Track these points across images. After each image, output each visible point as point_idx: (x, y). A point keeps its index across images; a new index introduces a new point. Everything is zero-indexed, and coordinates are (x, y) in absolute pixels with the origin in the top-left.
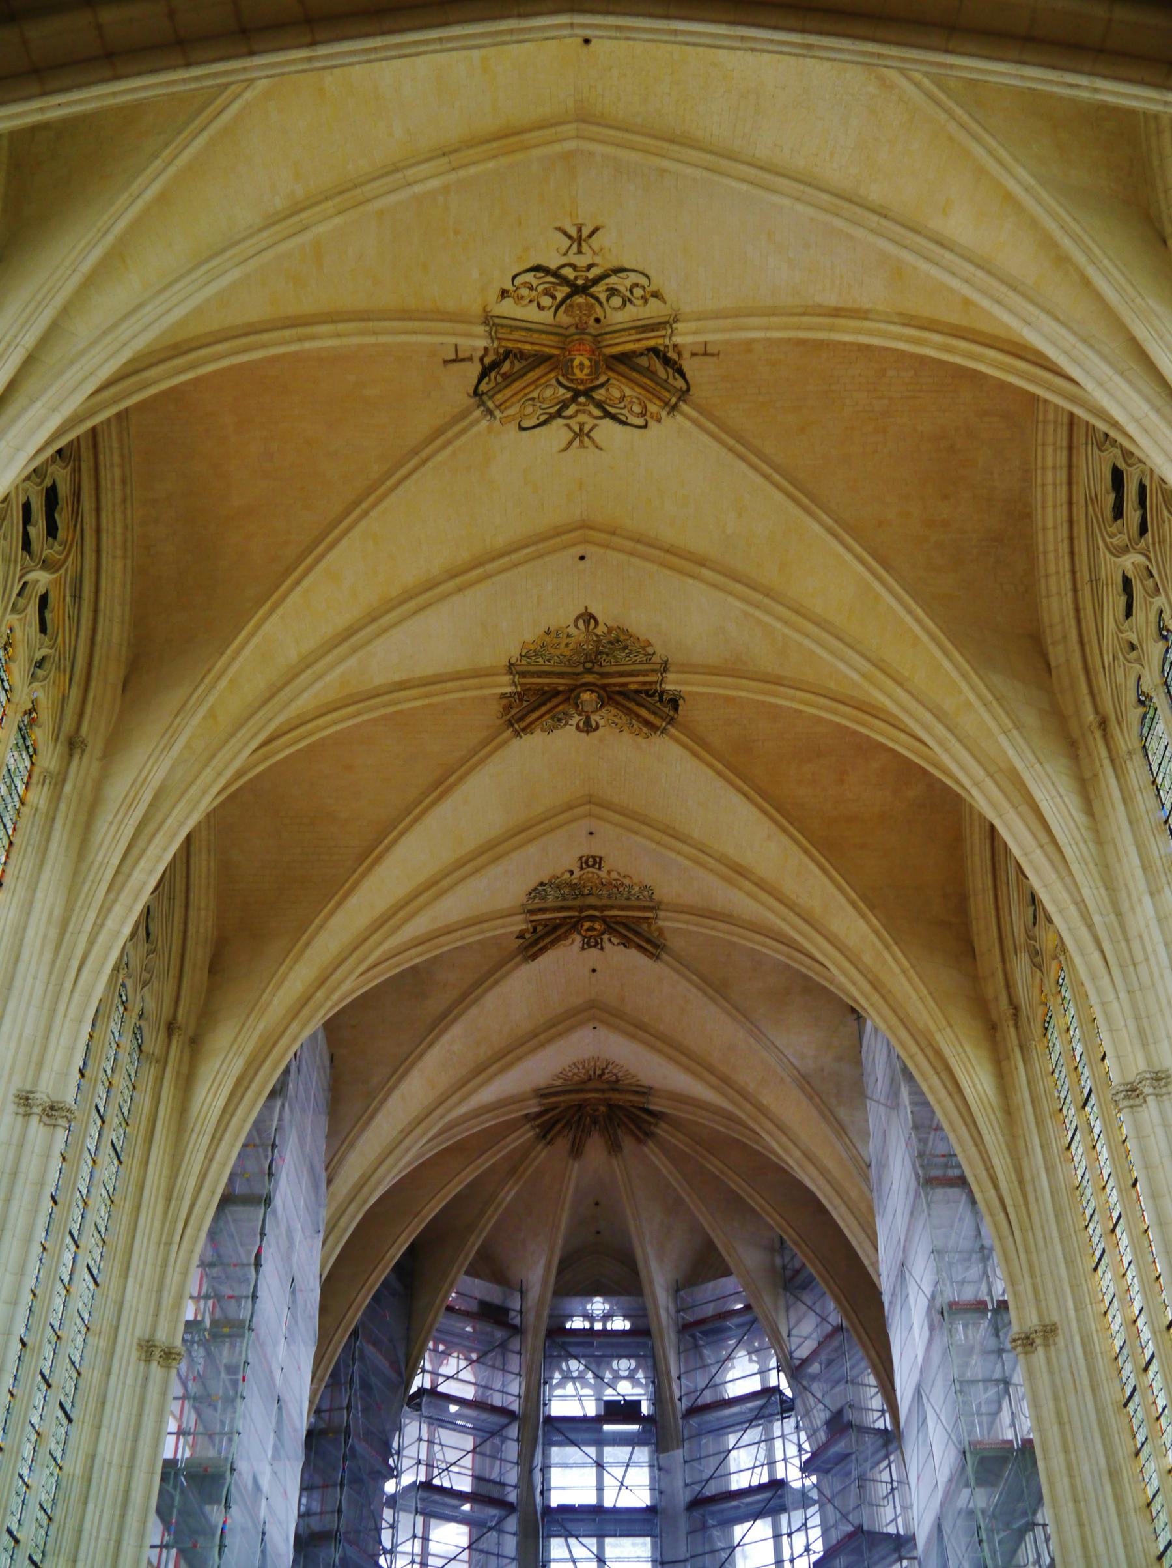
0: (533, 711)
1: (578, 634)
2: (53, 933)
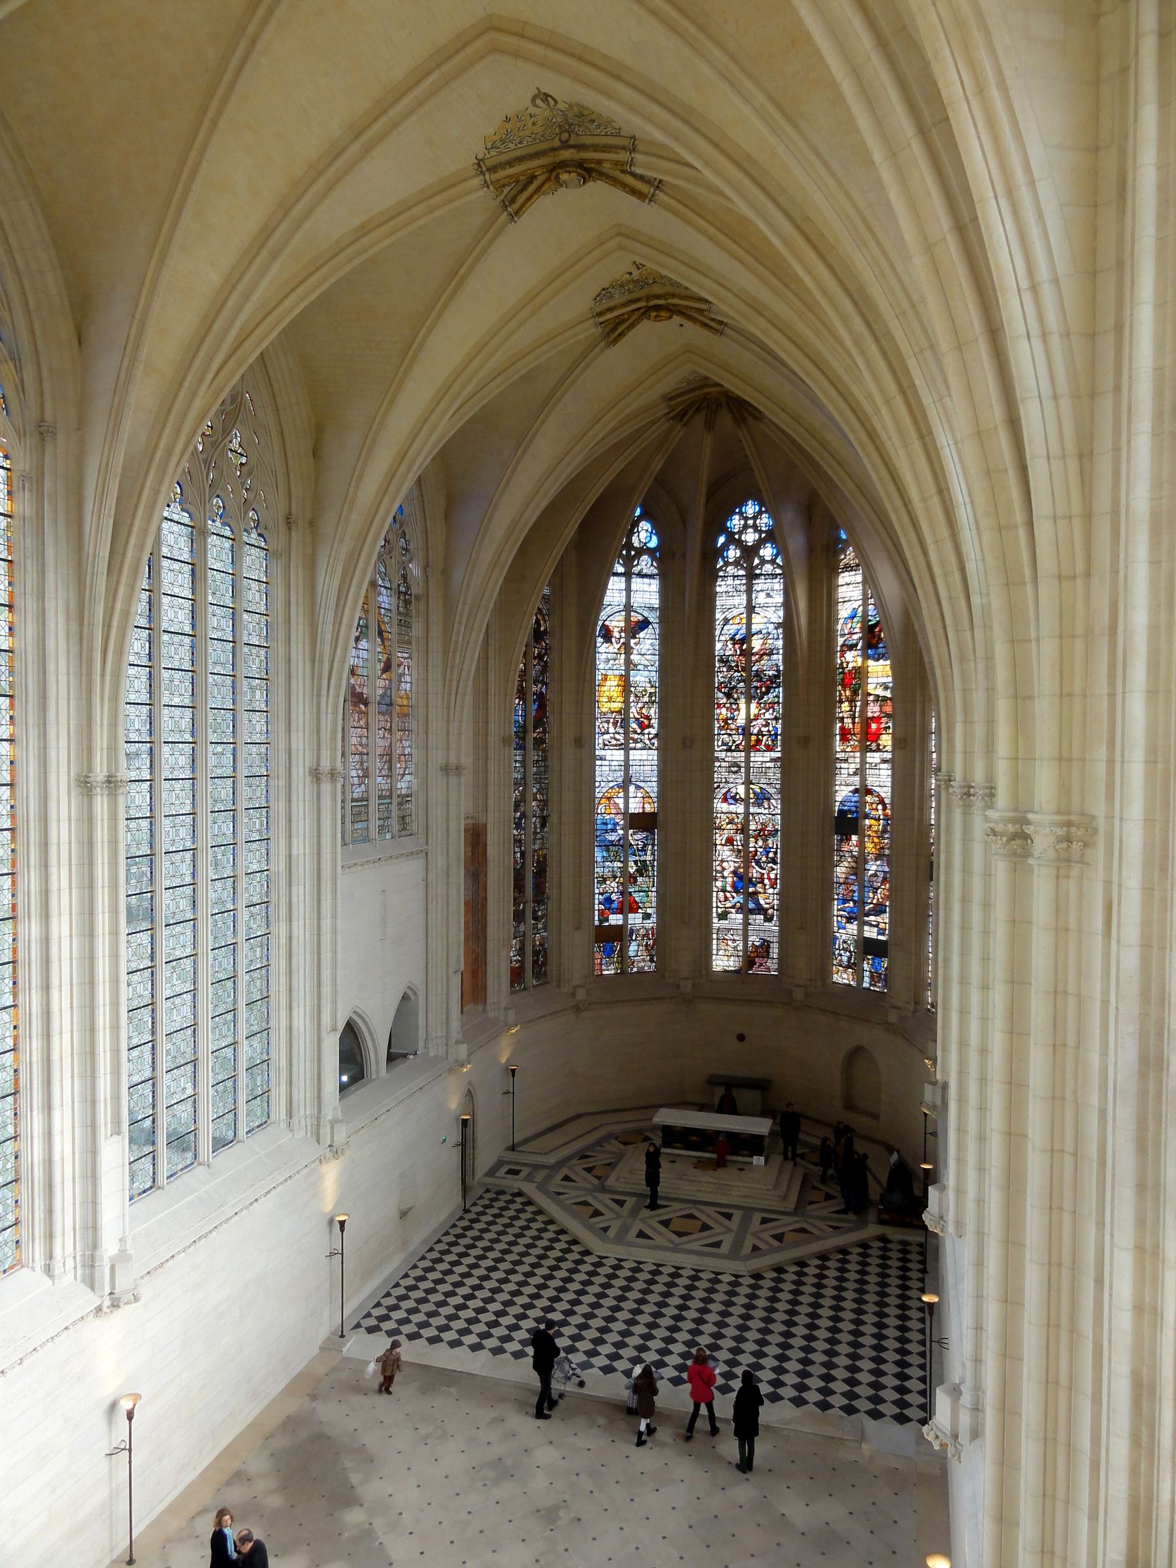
0: (521, 191)
1: (542, 111)
2: (74, 627)
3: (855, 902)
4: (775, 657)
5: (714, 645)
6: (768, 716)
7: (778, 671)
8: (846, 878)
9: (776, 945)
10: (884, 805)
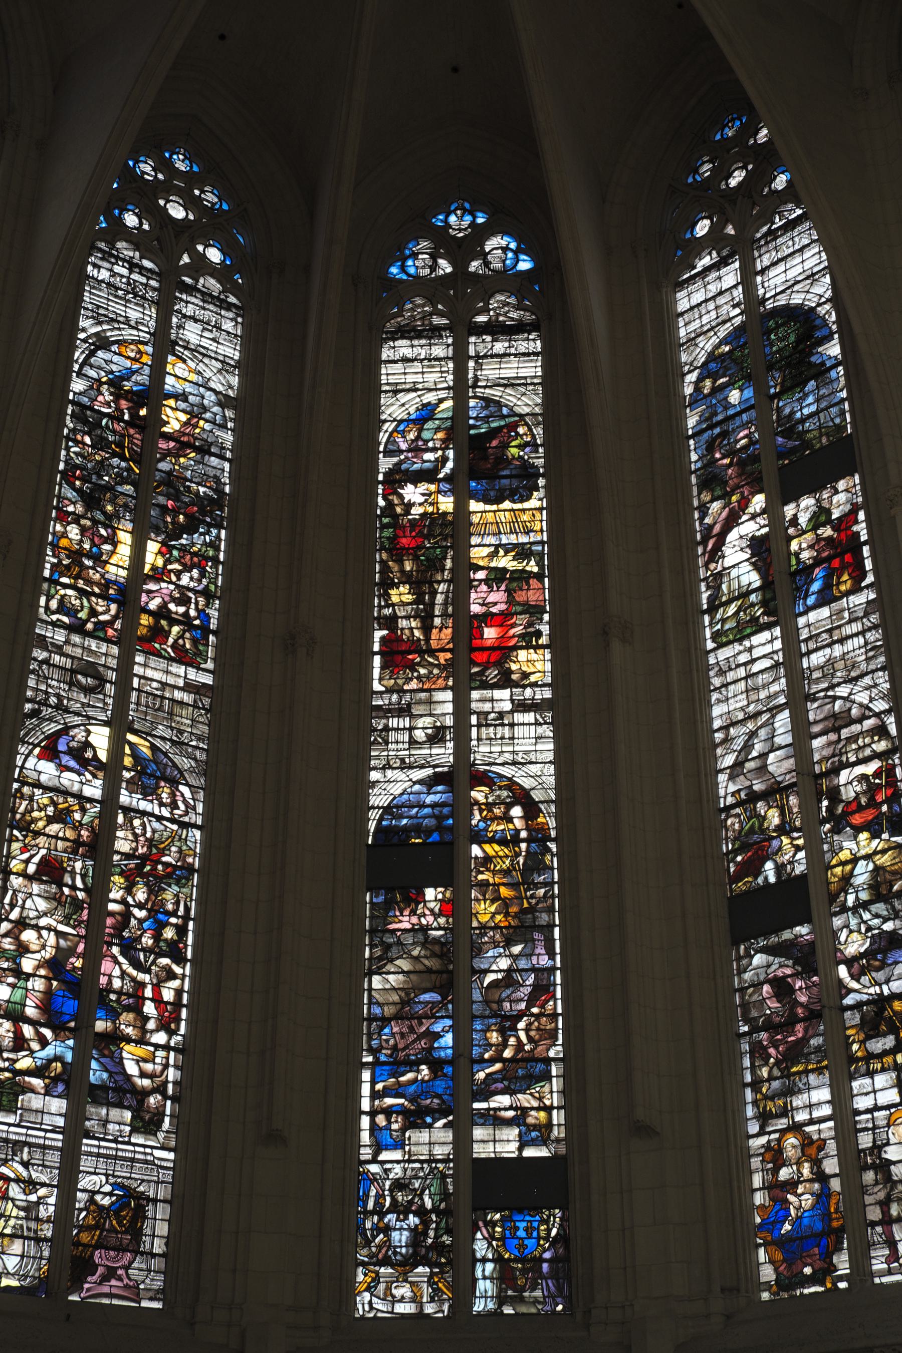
3: (436, 1066)
4: (214, 461)
5: (69, 380)
6: (185, 580)
7: (219, 491)
8: (403, 1003)
9: (162, 1212)
10: (531, 809)
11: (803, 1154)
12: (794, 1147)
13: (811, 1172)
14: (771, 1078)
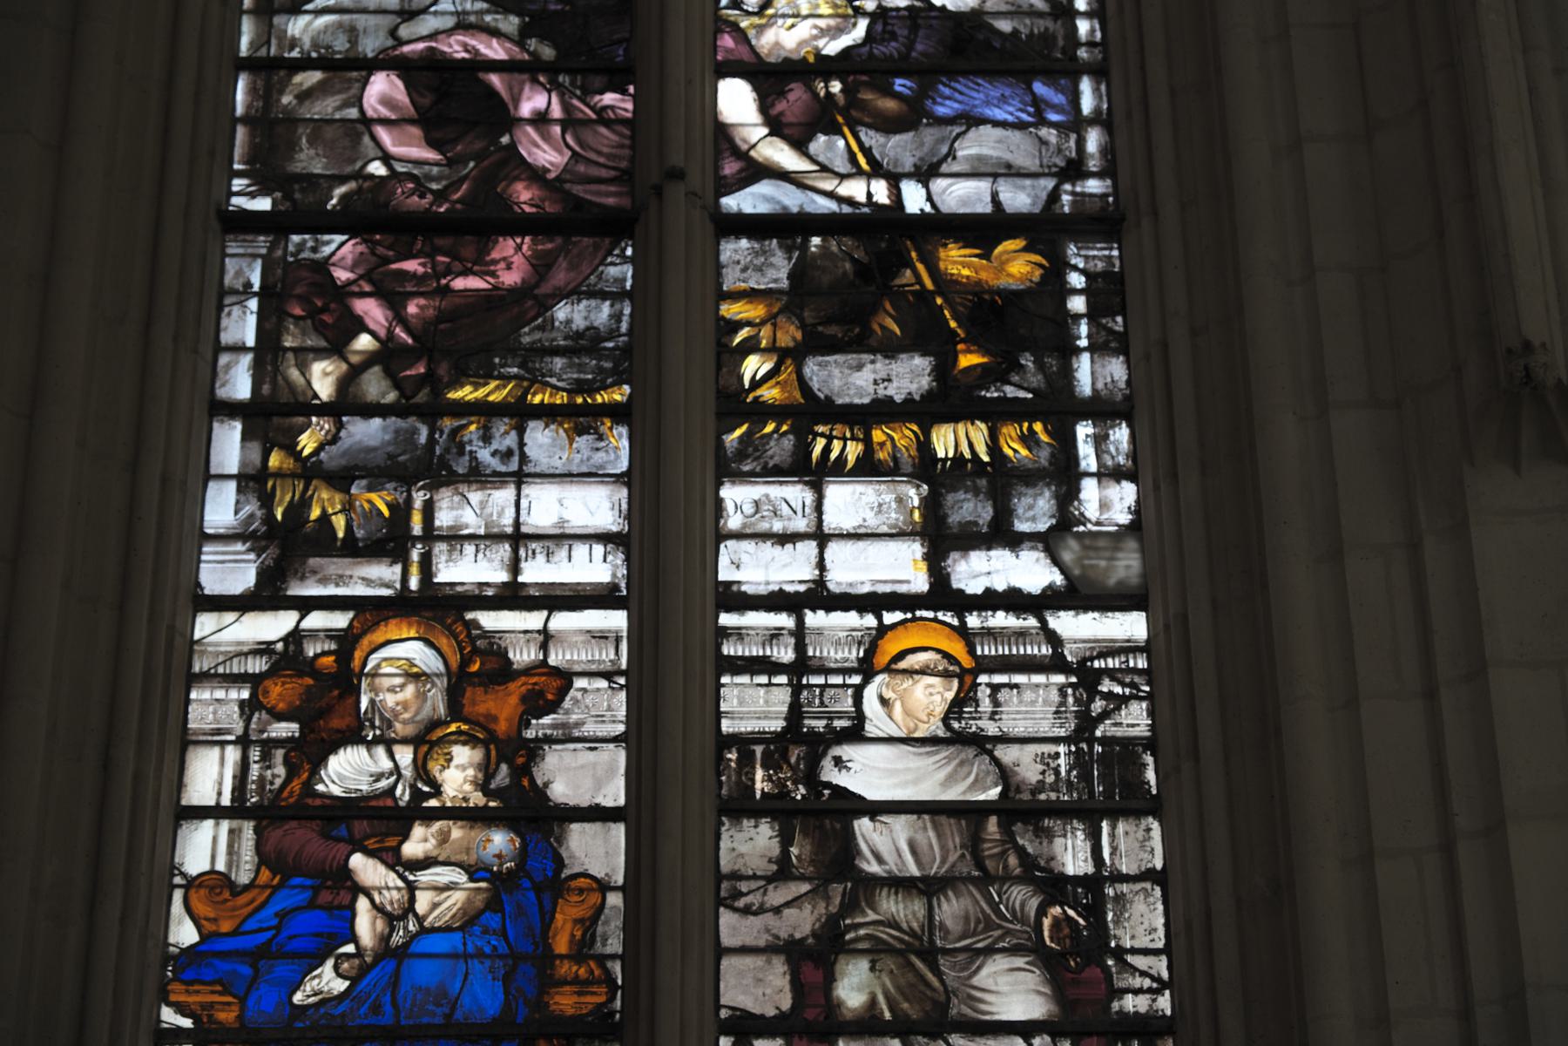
11: (455, 708)
12: (415, 676)
13: (484, 786)
14: (346, 405)
